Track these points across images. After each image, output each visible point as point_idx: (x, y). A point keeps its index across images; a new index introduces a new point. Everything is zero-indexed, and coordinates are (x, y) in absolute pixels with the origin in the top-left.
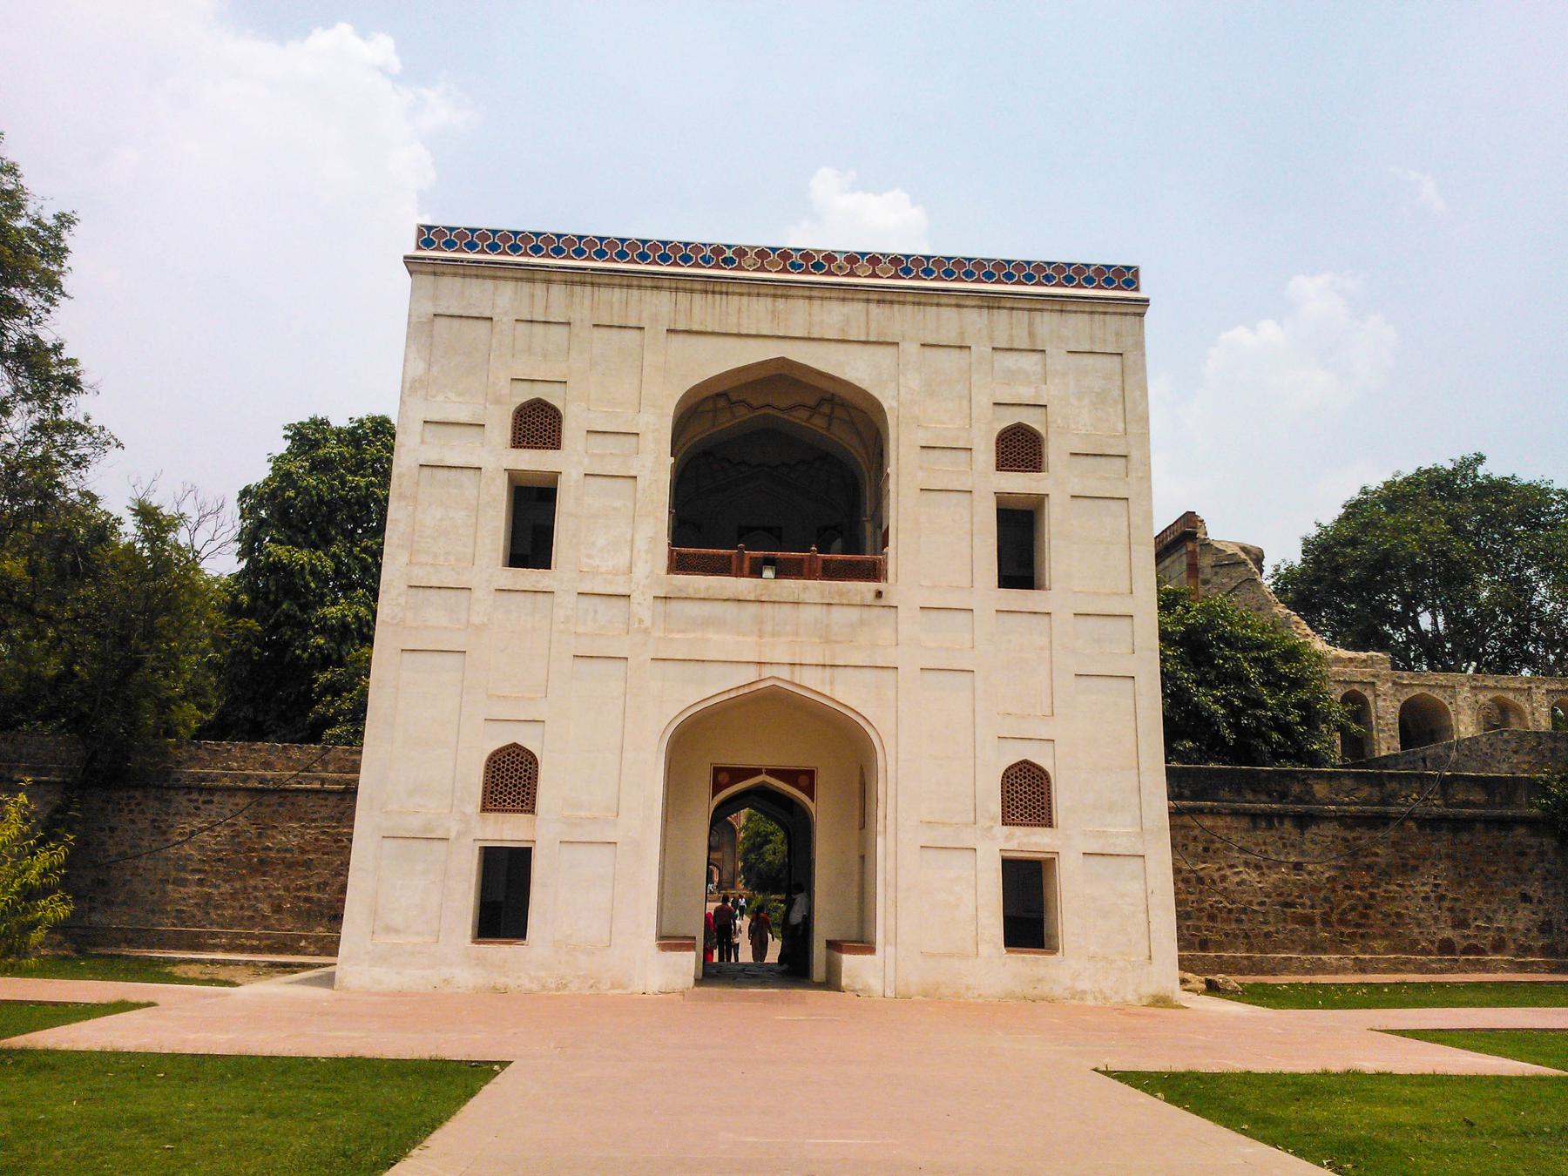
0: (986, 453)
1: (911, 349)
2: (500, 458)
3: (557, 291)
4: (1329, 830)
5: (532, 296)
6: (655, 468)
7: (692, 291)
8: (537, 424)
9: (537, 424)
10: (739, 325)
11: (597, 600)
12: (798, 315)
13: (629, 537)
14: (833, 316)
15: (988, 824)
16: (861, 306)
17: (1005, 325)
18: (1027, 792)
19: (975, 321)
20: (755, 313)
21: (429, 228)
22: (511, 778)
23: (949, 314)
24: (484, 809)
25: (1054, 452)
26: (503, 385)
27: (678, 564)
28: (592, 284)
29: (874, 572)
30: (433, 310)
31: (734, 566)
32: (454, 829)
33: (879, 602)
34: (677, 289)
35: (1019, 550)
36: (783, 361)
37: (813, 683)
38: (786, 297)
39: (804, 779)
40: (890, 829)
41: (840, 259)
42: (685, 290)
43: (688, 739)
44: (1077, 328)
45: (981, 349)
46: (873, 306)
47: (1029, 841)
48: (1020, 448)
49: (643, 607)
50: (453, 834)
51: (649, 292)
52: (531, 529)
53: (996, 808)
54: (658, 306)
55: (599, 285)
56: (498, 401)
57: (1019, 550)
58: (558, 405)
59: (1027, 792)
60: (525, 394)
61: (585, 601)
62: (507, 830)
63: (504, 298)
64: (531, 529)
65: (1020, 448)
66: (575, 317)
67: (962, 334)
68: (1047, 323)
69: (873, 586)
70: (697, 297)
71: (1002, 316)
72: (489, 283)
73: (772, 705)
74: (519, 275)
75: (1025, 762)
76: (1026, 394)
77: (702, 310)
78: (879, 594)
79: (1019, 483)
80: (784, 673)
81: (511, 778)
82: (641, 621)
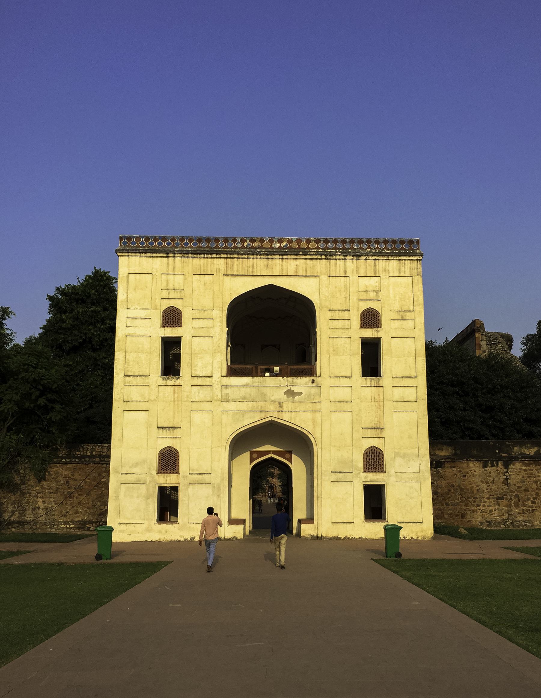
0: (356, 321)
1: (324, 278)
3: (178, 261)
4: (518, 465)
5: (168, 264)
6: (220, 330)
7: (233, 258)
9: (172, 317)
10: (253, 272)
11: (199, 387)
12: (277, 264)
13: (211, 362)
14: (292, 264)
15: (358, 472)
16: (304, 260)
17: (365, 265)
18: (374, 459)
19: (350, 264)
20: (259, 264)
21: (125, 237)
22: (169, 460)
23: (340, 263)
24: (159, 472)
26: (158, 302)
28: (192, 257)
29: (310, 372)
30: (128, 272)
31: (254, 372)
32: (148, 480)
33: (314, 384)
34: (227, 258)
35: (371, 360)
36: (271, 286)
38: (272, 258)
40: (320, 475)
41: (294, 240)
42: (230, 258)
44: (392, 265)
45: (353, 278)
46: (308, 261)
47: (374, 478)
48: (370, 319)
49: (217, 392)
50: (148, 482)
51: (215, 259)
52: (171, 360)
53: (361, 465)
54: (219, 263)
55: (194, 257)
56: (156, 309)
57: (371, 360)
58: (180, 308)
59: (374, 459)
60: (166, 304)
61: (195, 389)
62: (169, 480)
64: (171, 360)
65: (370, 319)
66: (186, 272)
67: (345, 272)
68: (382, 264)
69: (312, 378)
70: (235, 260)
71: (361, 262)
72: (151, 259)
74: (162, 255)
75: (373, 446)
76: (372, 295)
77: (239, 264)
78: (313, 381)
80: (276, 414)
81: (169, 460)
82: (217, 396)
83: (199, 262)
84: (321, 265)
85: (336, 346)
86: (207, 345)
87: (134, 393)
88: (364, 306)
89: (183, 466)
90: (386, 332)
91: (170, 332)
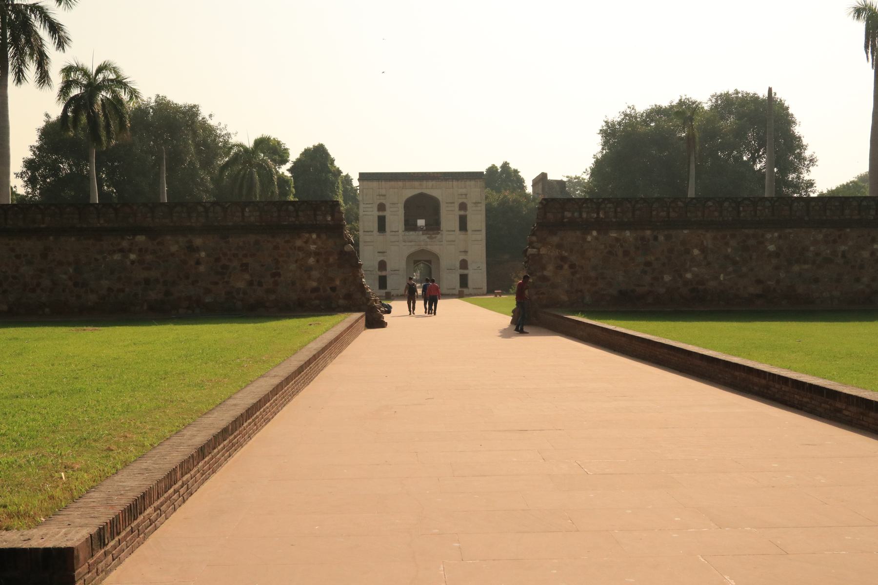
8: (382, 207)
9: (382, 207)
14: (430, 183)
18: (464, 264)
19: (455, 183)
20: (416, 184)
22: (382, 265)
25: (469, 206)
35: (463, 225)
39: (430, 262)
44: (473, 183)
48: (463, 207)
57: (463, 225)
59: (464, 264)
65: (463, 207)
73: (422, 251)
79: (462, 213)
81: (382, 265)
83: (392, 183)
84: (444, 184)
85: (449, 219)
86: (396, 219)
88: (461, 201)
89: (388, 268)
91: (381, 214)
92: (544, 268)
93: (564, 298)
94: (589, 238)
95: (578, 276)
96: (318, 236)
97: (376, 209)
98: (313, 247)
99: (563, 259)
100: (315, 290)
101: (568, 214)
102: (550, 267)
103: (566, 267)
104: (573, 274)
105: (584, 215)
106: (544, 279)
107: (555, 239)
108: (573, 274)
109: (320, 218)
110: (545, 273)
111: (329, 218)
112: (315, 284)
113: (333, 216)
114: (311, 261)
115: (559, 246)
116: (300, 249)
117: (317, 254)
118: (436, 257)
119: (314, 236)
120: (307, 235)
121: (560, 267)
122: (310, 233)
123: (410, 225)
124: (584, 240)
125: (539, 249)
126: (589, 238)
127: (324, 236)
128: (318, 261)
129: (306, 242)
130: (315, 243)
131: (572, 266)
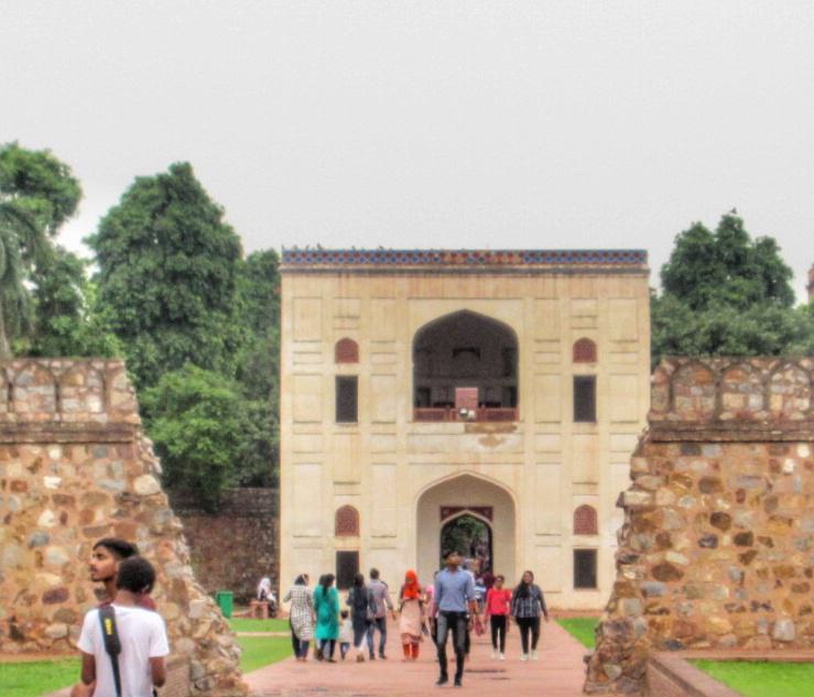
2: (332, 369)
9: (347, 351)
14: (490, 284)
20: (450, 284)
22: (347, 521)
27: (419, 417)
35: (584, 399)
37: (483, 472)
39: (487, 511)
43: (427, 497)
44: (614, 283)
48: (585, 351)
54: (403, 283)
57: (584, 399)
63: (326, 285)
65: (585, 351)
68: (601, 282)
73: (466, 482)
77: (425, 284)
79: (583, 369)
81: (347, 521)
84: (525, 285)
85: (543, 382)
86: (389, 380)
87: (306, 442)
90: (603, 370)
92: (665, 543)
93: (720, 622)
94: (788, 465)
95: (757, 565)
96: (67, 455)
97: (330, 355)
98: (51, 482)
99: (718, 519)
100: (54, 596)
101: (732, 401)
102: (683, 541)
103: (726, 539)
104: (746, 559)
105: (776, 404)
106: (665, 572)
107: (698, 467)
108: (746, 559)
109: (68, 404)
110: (672, 557)
111: (95, 404)
112: (54, 580)
113: (105, 399)
114: (47, 518)
115: (709, 485)
116: (17, 486)
117: (62, 500)
118: (504, 496)
119: (55, 452)
120: (37, 451)
121: (713, 542)
122: (45, 443)
123: (431, 401)
124: (775, 468)
125: (652, 492)
126: (788, 465)
127: (79, 452)
128: (64, 520)
129: (34, 468)
130: (56, 472)
131: (743, 539)
